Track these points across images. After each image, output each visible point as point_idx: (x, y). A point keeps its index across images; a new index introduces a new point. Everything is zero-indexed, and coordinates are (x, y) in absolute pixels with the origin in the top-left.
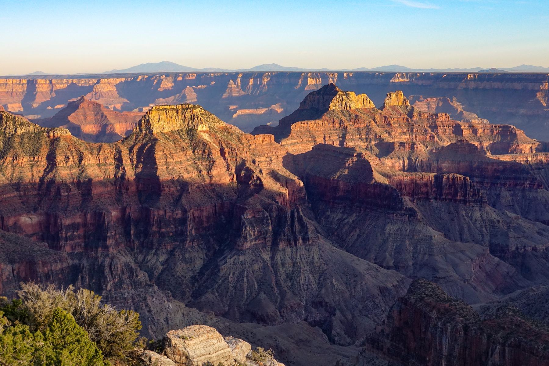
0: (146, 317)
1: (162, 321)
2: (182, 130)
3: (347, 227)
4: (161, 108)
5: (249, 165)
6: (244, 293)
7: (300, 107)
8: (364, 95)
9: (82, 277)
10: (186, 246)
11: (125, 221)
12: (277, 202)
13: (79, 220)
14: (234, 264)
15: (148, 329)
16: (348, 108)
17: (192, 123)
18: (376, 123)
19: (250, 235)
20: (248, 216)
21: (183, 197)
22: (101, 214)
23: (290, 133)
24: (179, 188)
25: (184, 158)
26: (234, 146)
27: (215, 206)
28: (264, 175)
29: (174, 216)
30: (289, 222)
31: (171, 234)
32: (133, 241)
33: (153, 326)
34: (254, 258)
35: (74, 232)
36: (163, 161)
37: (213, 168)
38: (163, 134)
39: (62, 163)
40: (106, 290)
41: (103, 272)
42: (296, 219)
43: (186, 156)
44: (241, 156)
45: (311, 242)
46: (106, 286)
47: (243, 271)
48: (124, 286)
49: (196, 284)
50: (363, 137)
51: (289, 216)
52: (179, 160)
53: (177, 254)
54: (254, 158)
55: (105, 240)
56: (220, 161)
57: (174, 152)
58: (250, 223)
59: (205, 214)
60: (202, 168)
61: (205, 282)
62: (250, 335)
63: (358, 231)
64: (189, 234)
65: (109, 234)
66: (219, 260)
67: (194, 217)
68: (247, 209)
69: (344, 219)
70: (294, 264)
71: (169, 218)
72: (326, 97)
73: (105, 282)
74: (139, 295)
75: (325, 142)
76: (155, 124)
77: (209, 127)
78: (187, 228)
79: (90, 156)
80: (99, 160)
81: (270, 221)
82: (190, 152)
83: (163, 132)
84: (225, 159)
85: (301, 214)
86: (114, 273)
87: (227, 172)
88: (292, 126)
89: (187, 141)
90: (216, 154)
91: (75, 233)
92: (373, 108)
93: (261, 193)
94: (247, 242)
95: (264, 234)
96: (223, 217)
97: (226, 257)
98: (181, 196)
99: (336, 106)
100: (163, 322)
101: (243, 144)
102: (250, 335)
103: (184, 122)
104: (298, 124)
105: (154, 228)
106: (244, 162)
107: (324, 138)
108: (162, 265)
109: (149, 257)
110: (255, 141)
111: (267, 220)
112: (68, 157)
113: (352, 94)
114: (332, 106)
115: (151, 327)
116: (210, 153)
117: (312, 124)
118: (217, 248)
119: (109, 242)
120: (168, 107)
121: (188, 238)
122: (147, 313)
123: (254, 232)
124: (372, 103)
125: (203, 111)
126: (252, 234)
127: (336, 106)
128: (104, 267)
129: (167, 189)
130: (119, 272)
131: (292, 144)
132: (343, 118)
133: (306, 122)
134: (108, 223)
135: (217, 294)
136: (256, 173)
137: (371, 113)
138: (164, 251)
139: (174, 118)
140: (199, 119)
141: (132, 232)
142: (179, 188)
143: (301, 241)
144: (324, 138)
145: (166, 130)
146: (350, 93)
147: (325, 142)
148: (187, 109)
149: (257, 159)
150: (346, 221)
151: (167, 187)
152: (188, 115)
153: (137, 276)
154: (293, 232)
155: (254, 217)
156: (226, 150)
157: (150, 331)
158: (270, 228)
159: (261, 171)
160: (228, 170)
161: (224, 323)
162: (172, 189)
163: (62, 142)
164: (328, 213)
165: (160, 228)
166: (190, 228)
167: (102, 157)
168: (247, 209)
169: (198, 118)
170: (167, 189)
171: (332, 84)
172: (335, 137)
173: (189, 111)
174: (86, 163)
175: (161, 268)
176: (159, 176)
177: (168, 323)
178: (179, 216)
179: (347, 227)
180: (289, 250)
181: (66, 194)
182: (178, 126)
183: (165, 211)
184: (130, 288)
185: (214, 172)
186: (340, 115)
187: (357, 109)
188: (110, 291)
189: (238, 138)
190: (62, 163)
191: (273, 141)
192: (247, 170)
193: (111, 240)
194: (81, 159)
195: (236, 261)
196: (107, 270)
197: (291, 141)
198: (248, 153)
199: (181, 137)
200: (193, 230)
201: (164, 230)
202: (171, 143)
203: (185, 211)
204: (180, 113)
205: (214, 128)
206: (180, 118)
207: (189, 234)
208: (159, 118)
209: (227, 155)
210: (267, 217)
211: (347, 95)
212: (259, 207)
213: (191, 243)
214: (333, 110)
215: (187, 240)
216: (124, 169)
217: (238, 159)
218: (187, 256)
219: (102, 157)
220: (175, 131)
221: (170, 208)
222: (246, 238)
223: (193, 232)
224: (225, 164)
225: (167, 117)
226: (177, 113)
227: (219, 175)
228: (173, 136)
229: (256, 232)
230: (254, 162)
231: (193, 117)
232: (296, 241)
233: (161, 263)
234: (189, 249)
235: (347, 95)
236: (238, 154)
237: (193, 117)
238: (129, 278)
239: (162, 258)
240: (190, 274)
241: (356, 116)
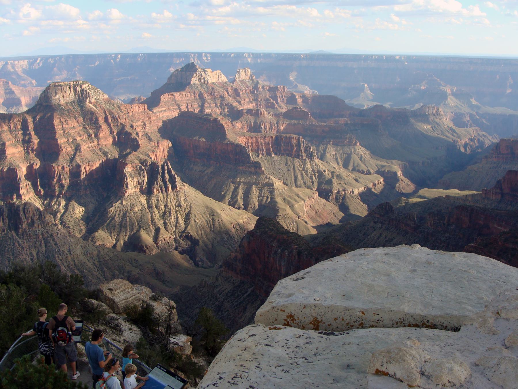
0: (54, 249)
1: (66, 252)
3: (206, 177)
4: (57, 84)
5: (128, 129)
8: (219, 72)
9: (3, 219)
11: (31, 175)
12: (151, 158)
15: (55, 258)
16: (206, 82)
18: (228, 94)
20: (128, 170)
21: (77, 155)
23: (160, 103)
25: (76, 124)
26: (116, 114)
28: (140, 136)
33: (59, 256)
34: (134, 202)
37: (100, 132)
40: (22, 229)
41: (19, 215)
42: (166, 172)
43: (78, 122)
44: (121, 122)
45: (178, 189)
46: (22, 226)
48: (36, 225)
49: (90, 224)
50: (218, 105)
51: (160, 170)
54: (131, 123)
56: (104, 126)
60: (90, 131)
61: (97, 222)
62: (134, 261)
63: (215, 180)
66: (106, 205)
68: (127, 164)
69: (204, 171)
70: (166, 206)
72: (188, 74)
73: (20, 223)
74: (47, 232)
75: (188, 110)
77: (96, 99)
82: (81, 119)
84: (109, 125)
85: (170, 167)
86: (27, 215)
88: (162, 97)
89: (79, 110)
90: (101, 121)
92: (226, 82)
93: (138, 151)
96: (109, 171)
97: (112, 202)
98: (75, 154)
100: (67, 253)
101: (122, 113)
102: (134, 261)
103: (75, 96)
104: (166, 95)
106: (123, 126)
107: (187, 107)
110: (132, 110)
111: (143, 173)
113: (209, 71)
114: (193, 80)
115: (58, 257)
116: (97, 119)
117: (177, 95)
118: (105, 195)
120: (63, 84)
121: (82, 188)
122: (54, 246)
124: (225, 77)
125: (90, 86)
128: (19, 211)
130: (31, 215)
131: (161, 111)
132: (202, 90)
133: (173, 93)
136: (134, 135)
137: (224, 86)
139: (68, 92)
141: (39, 183)
142: (74, 148)
143: (170, 188)
144: (187, 107)
146: (207, 70)
147: (188, 110)
148: (78, 85)
149: (134, 124)
150: (206, 172)
152: (79, 89)
153: (45, 218)
154: (164, 182)
156: (109, 116)
157: (57, 259)
158: (146, 179)
159: (137, 134)
160: (111, 133)
161: (113, 253)
162: (68, 149)
164: (191, 166)
167: (12, 125)
168: (127, 164)
169: (86, 91)
170: (64, 150)
171: (193, 63)
172: (196, 105)
176: (57, 139)
177: (70, 253)
179: (206, 177)
180: (161, 195)
184: (40, 226)
185: (101, 135)
186: (200, 87)
187: (213, 83)
188: (25, 229)
189: (119, 108)
191: (146, 110)
196: (22, 213)
197: (160, 109)
198: (127, 119)
204: (72, 89)
205: (99, 99)
209: (110, 121)
211: (205, 71)
212: (137, 162)
214: (194, 84)
217: (119, 124)
219: (12, 125)
223: (86, 183)
226: (70, 88)
227: (105, 138)
229: (135, 183)
230: (132, 127)
231: (83, 91)
232: (166, 188)
235: (205, 71)
236: (119, 120)
238: (39, 219)
241: (213, 89)
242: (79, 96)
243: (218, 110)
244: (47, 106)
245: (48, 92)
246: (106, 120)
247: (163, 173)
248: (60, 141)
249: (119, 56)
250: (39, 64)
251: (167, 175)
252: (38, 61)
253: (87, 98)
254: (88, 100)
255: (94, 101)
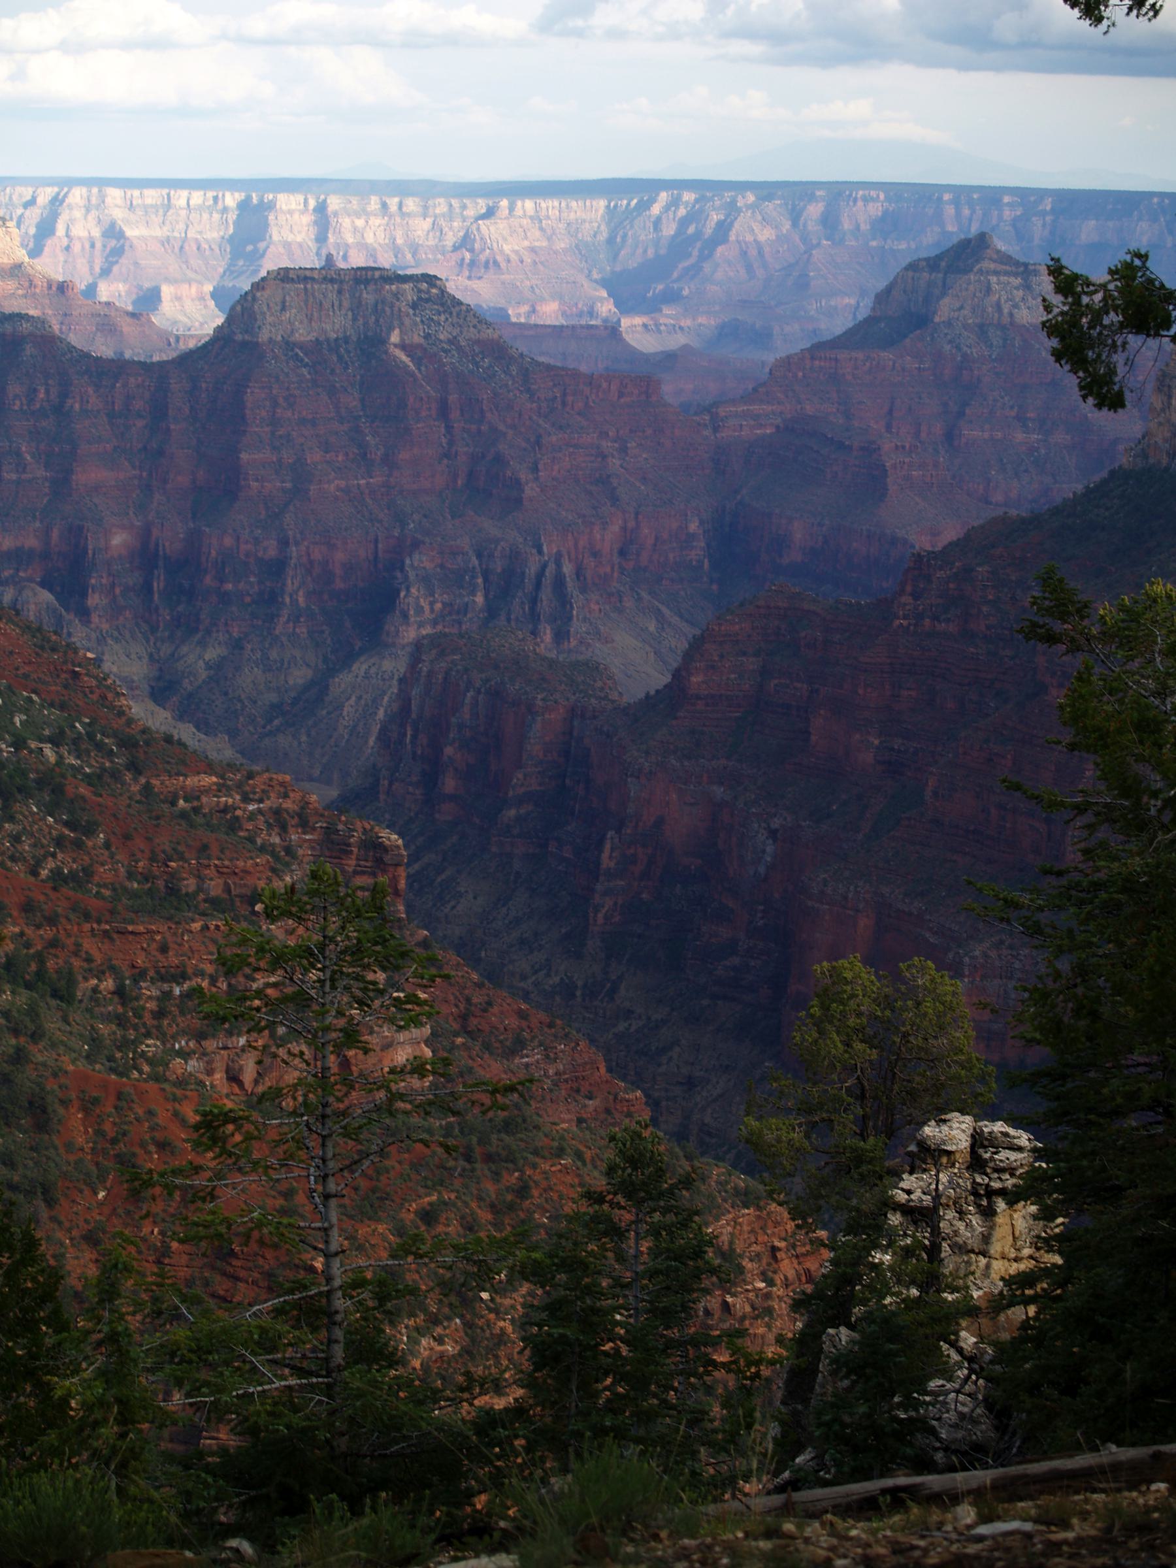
2: (346, 340)
6: (366, 742)
7: (873, 309)
10: (277, 632)
11: (146, 556)
13: (32, 542)
14: (367, 676)
17: (377, 321)
19: (420, 610)
22: (81, 528)
24: (288, 485)
27: (376, 541)
29: (260, 554)
30: (529, 585)
31: (248, 599)
32: (157, 609)
35: (18, 570)
36: (264, 414)
38: (288, 345)
39: (18, 402)
45: (573, 643)
47: (384, 692)
52: (310, 417)
53: (249, 646)
55: (84, 595)
57: (297, 392)
58: (426, 580)
59: (340, 556)
64: (288, 600)
65: (93, 581)
67: (311, 562)
71: (247, 555)
76: (270, 319)
78: (284, 585)
79: (90, 391)
80: (113, 403)
81: (480, 581)
83: (292, 339)
87: (445, 461)
91: (22, 574)
94: (408, 624)
95: (458, 613)
99: (962, 308)
103: (355, 319)
105: (208, 580)
108: (208, 666)
109: (185, 649)
111: (473, 577)
112: (35, 390)
114: (945, 309)
119: (94, 600)
121: (285, 613)
123: (432, 604)
126: (427, 608)
127: (962, 308)
129: (255, 484)
134: (94, 554)
135: (304, 738)
138: (221, 638)
139: (327, 305)
140: (396, 309)
145: (303, 334)
148: (367, 282)
151: (257, 480)
152: (368, 297)
153: (69, 635)
155: (442, 566)
156: (453, 398)
158: (479, 599)
163: (29, 350)
165: (222, 581)
166: (296, 590)
173: (371, 287)
174: (77, 406)
175: (203, 674)
178: (272, 553)
181: (14, 476)
182: (337, 326)
183: (238, 539)
190: (18, 402)
192: (499, 459)
193: (97, 596)
194: (64, 395)
195: (373, 670)
199: (340, 358)
200: (301, 593)
201: (229, 587)
202: (305, 371)
203: (284, 543)
206: (346, 304)
207: (288, 600)
208: (284, 302)
209: (455, 415)
210: (474, 568)
213: (291, 624)
214: (949, 324)
215: (278, 616)
216: (168, 429)
218: (274, 654)
220: (328, 340)
221: (252, 531)
222: (405, 616)
223: (301, 600)
224: (444, 441)
225: (306, 302)
226: (340, 292)
228: (318, 353)
229: (438, 606)
233: (207, 664)
234: (284, 639)
237: (379, 307)
239: (212, 654)
240: (273, 697)
242: (366, 324)
243: (1020, 436)
244: (244, 344)
245: (254, 299)
246: (444, 410)
247: (538, 585)
248: (244, 456)
249: (1048, 205)
250: (657, 223)
251: (546, 595)
252: (656, 209)
253: (391, 329)
254: (395, 338)
255: (417, 339)
